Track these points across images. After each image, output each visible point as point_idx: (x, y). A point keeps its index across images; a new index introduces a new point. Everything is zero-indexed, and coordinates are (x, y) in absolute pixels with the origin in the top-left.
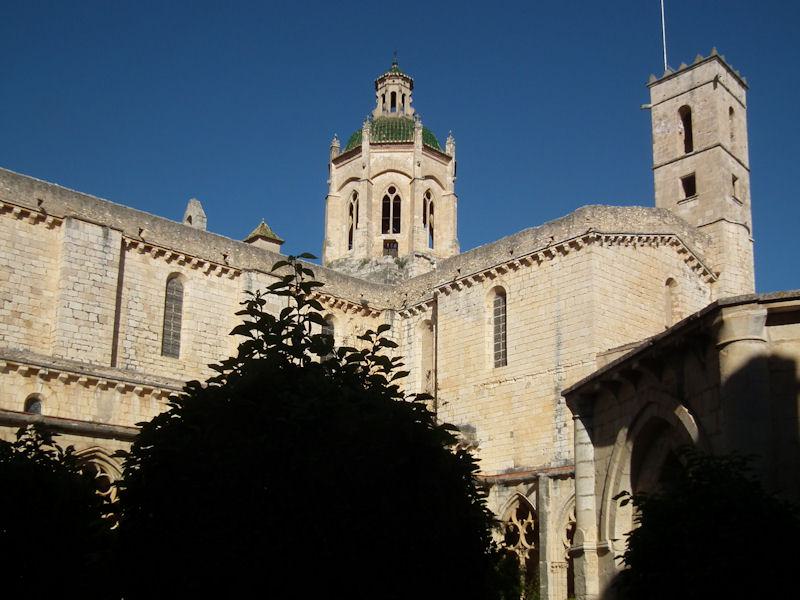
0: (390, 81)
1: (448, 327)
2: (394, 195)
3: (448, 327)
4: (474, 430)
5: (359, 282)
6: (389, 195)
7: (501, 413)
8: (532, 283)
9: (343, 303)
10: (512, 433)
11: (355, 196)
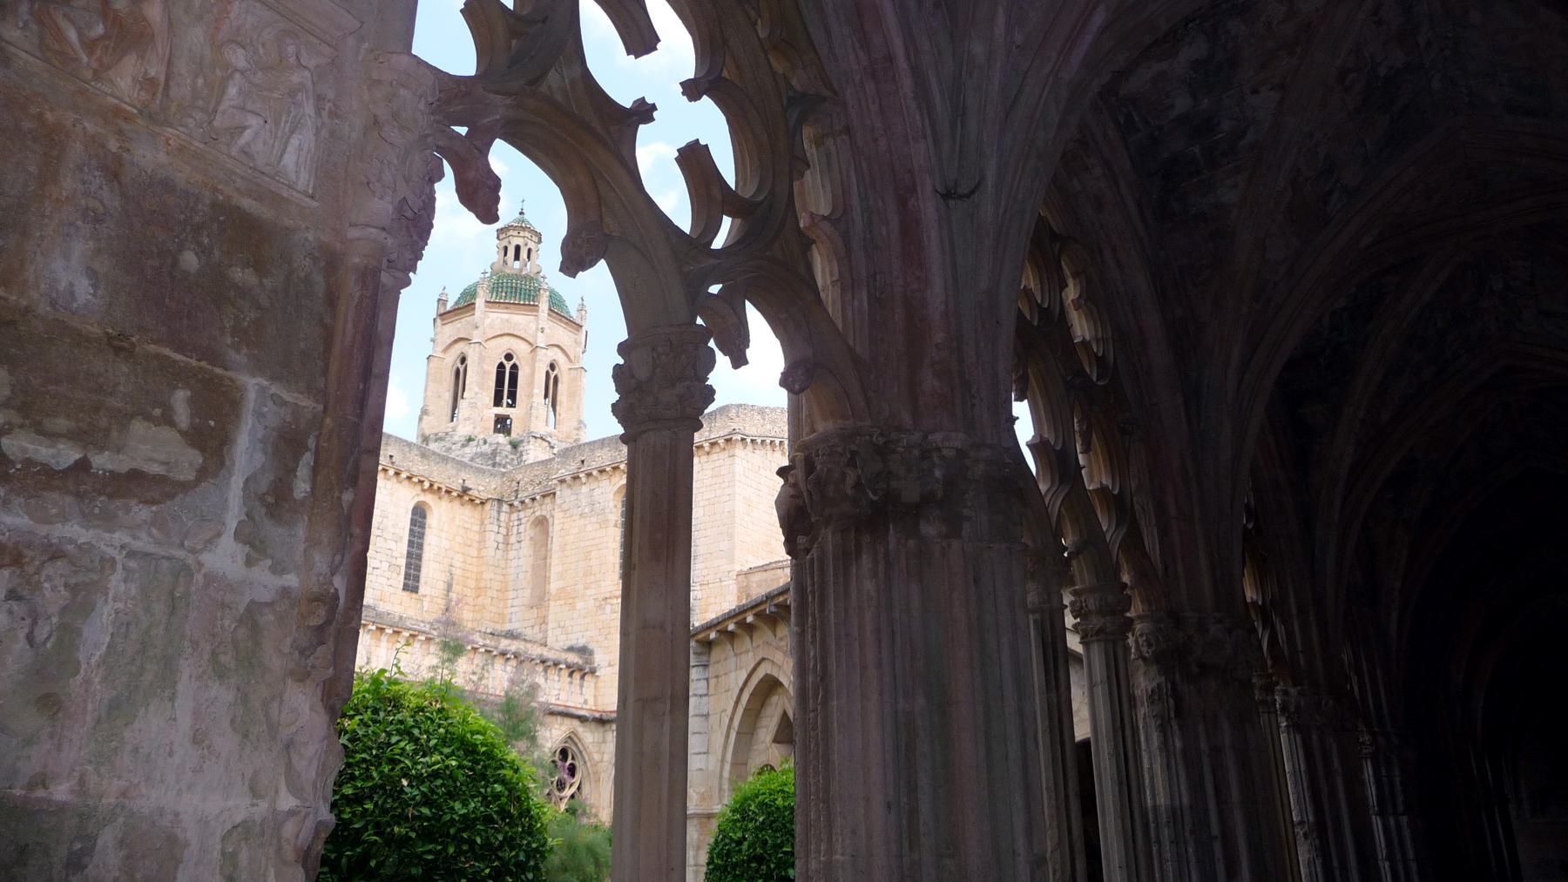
0: (515, 233)
1: (566, 526)
2: (511, 363)
3: (566, 526)
4: (591, 653)
5: (461, 465)
6: (505, 362)
9: (439, 488)
11: (463, 360)
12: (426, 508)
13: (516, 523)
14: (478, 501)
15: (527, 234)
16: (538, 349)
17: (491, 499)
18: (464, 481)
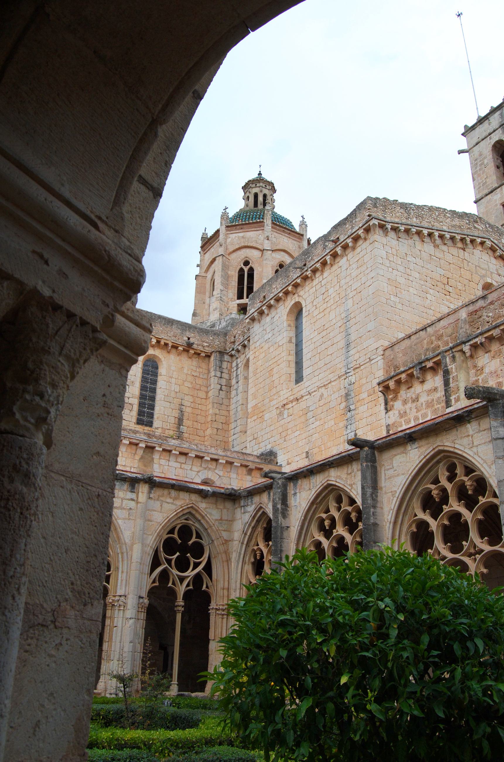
0: (254, 185)
2: (248, 267)
6: (244, 267)
7: (298, 433)
8: (323, 290)
10: (307, 453)
12: (157, 360)
13: (235, 369)
14: (203, 354)
15: (261, 184)
16: (264, 251)
17: (213, 352)
18: (189, 339)
